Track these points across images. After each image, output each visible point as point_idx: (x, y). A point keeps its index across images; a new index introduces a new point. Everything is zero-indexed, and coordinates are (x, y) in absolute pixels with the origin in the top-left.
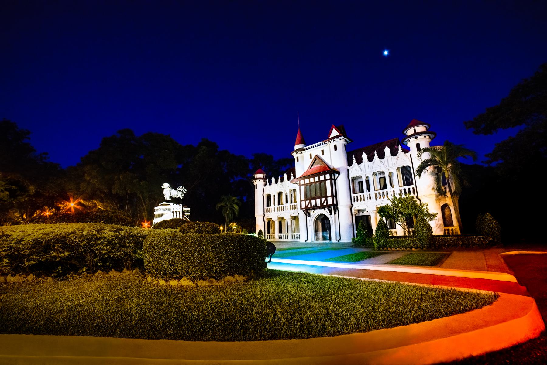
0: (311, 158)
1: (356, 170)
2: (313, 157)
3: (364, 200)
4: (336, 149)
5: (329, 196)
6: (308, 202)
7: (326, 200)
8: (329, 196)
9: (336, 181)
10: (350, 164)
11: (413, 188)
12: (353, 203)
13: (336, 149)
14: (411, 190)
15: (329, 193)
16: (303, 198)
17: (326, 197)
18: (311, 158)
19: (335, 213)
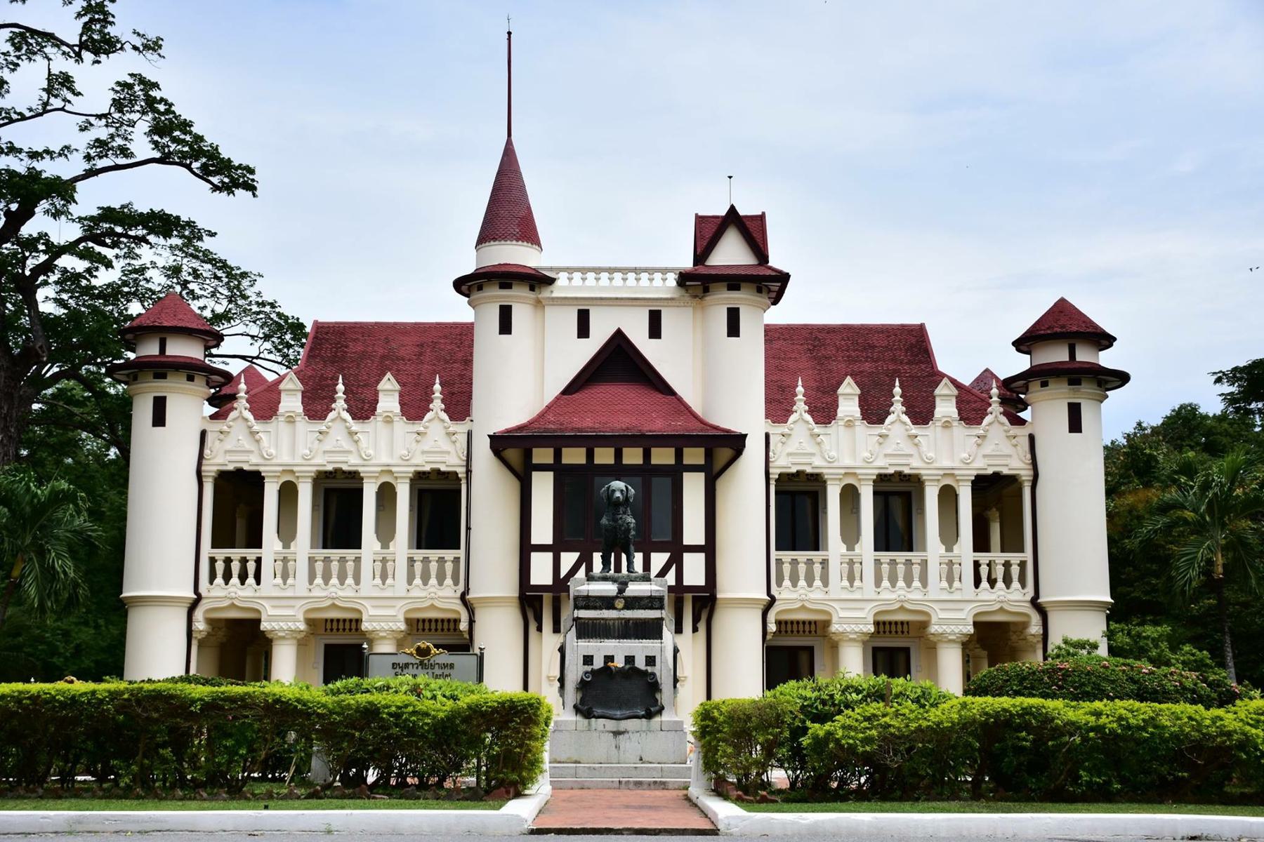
0: (583, 331)
1: (802, 445)
2: (600, 333)
3: (825, 581)
4: (734, 330)
5: (694, 549)
6: (569, 559)
7: (676, 561)
8: (694, 549)
9: (721, 484)
10: (778, 408)
11: (1022, 565)
12: (774, 591)
13: (734, 330)
14: (1015, 570)
15: (693, 532)
16: (542, 532)
17: (677, 551)
18: (583, 331)
19: (695, 630)
